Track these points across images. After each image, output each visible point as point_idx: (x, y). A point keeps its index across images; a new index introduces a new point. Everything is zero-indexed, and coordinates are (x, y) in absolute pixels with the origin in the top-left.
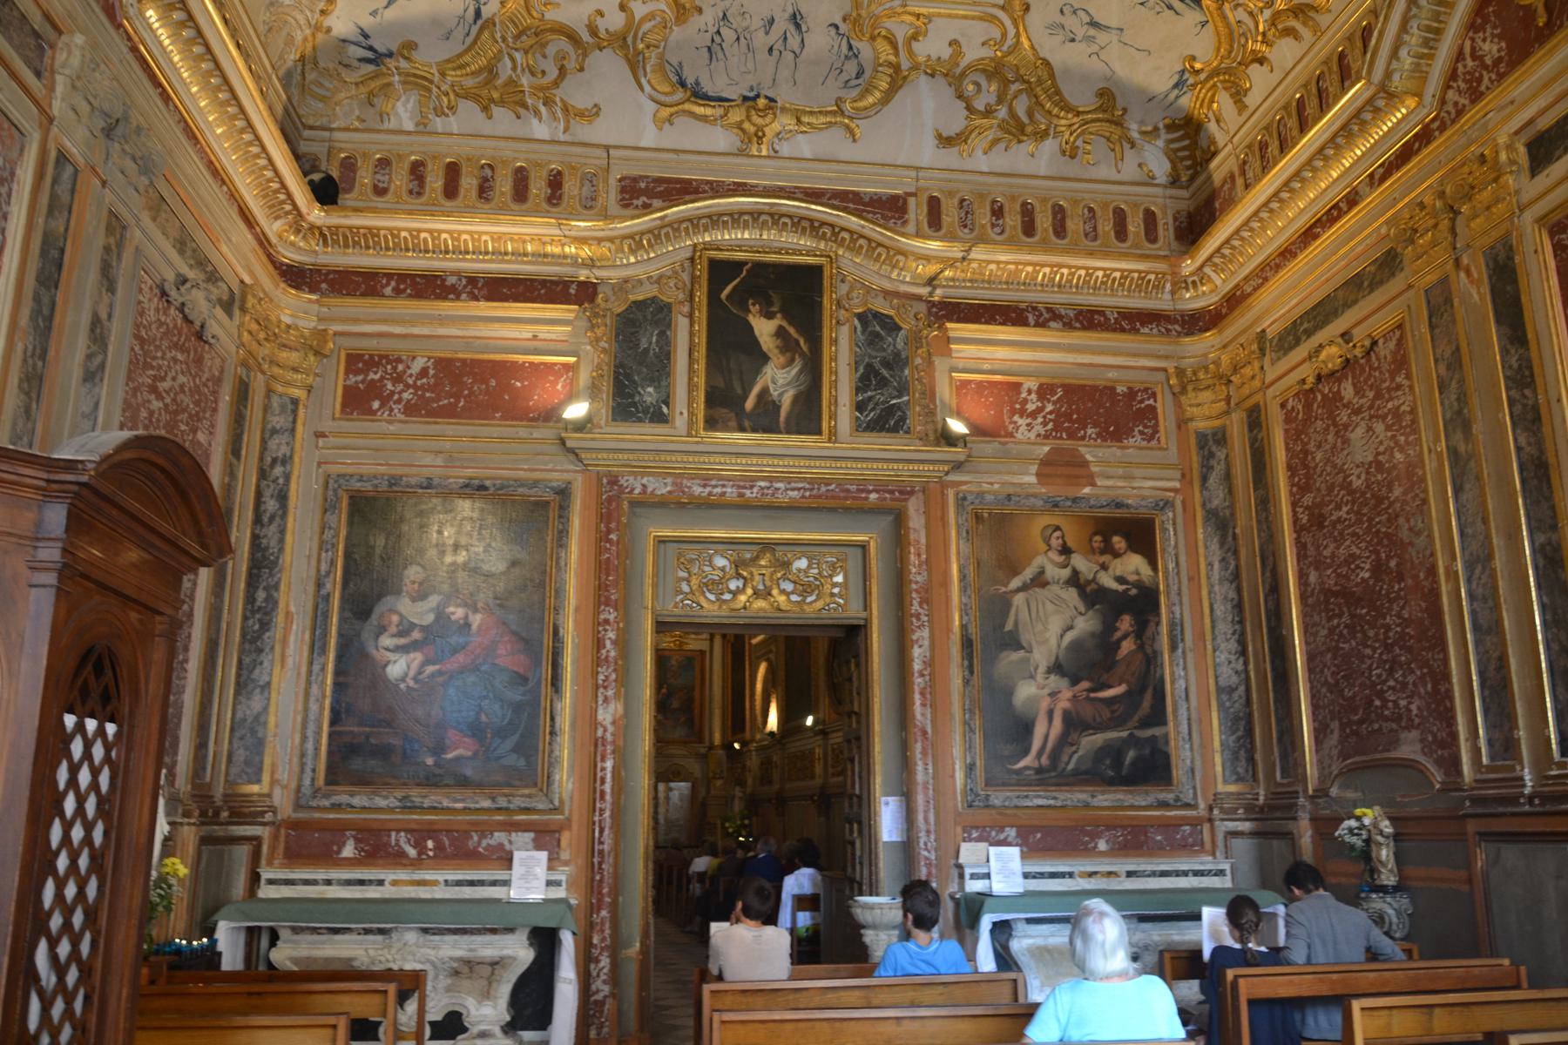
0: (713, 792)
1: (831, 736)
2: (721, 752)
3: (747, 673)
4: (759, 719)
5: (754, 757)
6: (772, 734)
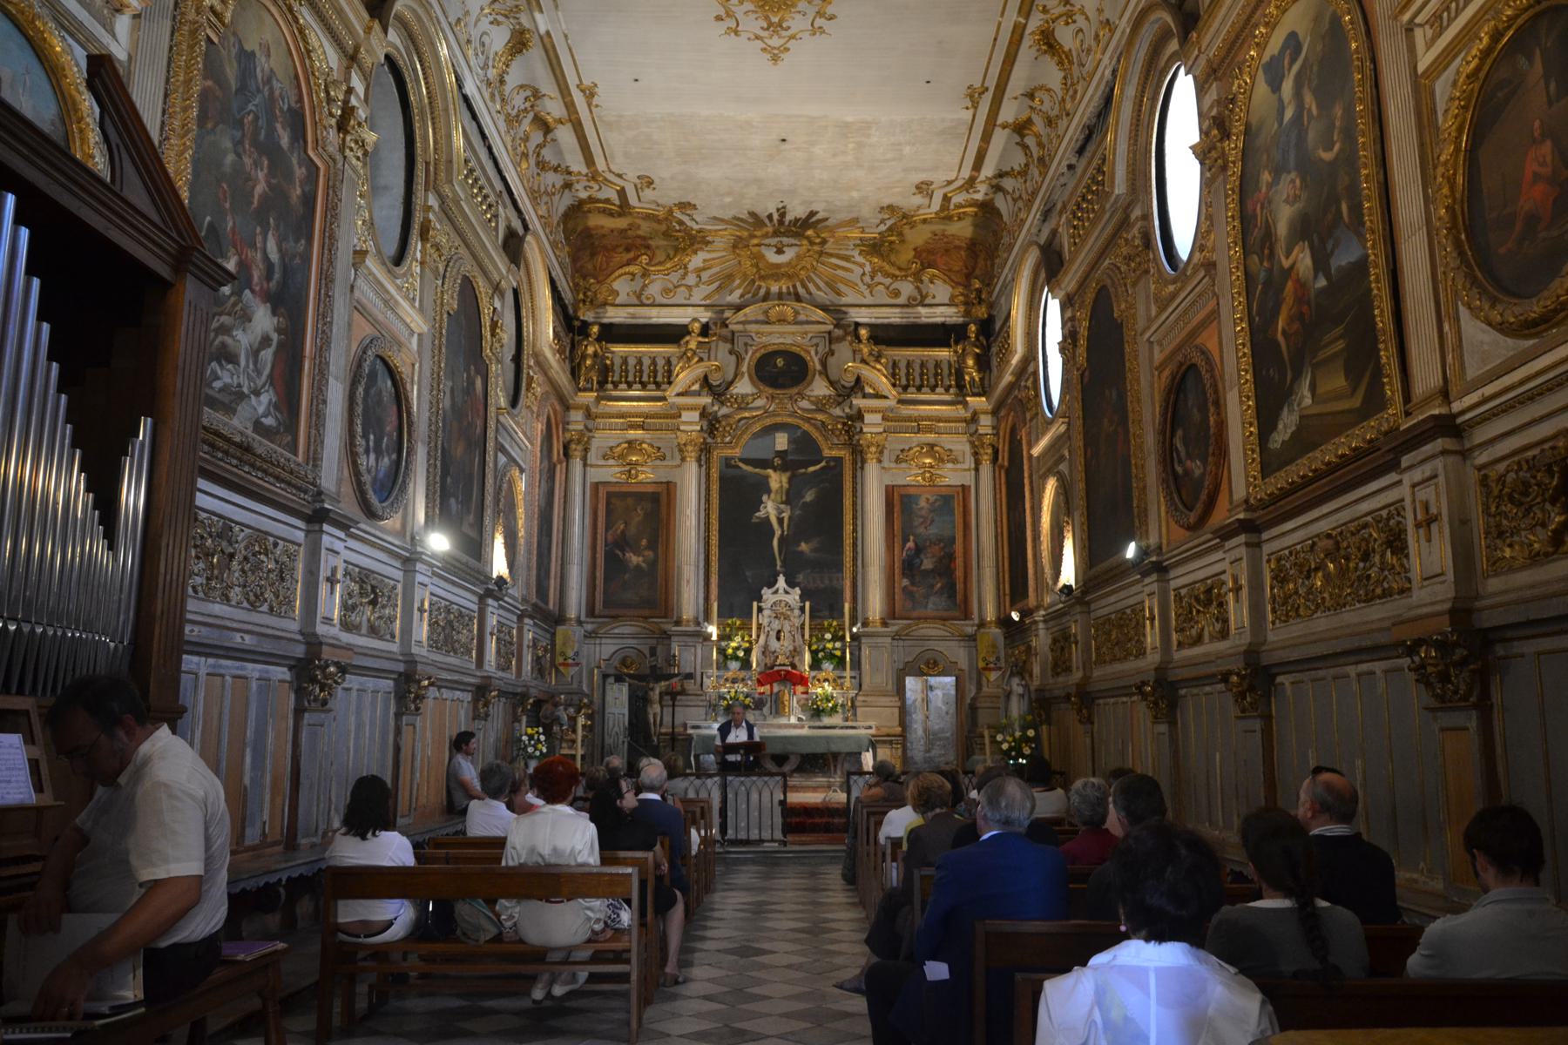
0: (985, 689)
1: (1172, 574)
2: (997, 630)
3: (1028, 506)
4: (1048, 571)
5: (1042, 632)
6: (1067, 588)
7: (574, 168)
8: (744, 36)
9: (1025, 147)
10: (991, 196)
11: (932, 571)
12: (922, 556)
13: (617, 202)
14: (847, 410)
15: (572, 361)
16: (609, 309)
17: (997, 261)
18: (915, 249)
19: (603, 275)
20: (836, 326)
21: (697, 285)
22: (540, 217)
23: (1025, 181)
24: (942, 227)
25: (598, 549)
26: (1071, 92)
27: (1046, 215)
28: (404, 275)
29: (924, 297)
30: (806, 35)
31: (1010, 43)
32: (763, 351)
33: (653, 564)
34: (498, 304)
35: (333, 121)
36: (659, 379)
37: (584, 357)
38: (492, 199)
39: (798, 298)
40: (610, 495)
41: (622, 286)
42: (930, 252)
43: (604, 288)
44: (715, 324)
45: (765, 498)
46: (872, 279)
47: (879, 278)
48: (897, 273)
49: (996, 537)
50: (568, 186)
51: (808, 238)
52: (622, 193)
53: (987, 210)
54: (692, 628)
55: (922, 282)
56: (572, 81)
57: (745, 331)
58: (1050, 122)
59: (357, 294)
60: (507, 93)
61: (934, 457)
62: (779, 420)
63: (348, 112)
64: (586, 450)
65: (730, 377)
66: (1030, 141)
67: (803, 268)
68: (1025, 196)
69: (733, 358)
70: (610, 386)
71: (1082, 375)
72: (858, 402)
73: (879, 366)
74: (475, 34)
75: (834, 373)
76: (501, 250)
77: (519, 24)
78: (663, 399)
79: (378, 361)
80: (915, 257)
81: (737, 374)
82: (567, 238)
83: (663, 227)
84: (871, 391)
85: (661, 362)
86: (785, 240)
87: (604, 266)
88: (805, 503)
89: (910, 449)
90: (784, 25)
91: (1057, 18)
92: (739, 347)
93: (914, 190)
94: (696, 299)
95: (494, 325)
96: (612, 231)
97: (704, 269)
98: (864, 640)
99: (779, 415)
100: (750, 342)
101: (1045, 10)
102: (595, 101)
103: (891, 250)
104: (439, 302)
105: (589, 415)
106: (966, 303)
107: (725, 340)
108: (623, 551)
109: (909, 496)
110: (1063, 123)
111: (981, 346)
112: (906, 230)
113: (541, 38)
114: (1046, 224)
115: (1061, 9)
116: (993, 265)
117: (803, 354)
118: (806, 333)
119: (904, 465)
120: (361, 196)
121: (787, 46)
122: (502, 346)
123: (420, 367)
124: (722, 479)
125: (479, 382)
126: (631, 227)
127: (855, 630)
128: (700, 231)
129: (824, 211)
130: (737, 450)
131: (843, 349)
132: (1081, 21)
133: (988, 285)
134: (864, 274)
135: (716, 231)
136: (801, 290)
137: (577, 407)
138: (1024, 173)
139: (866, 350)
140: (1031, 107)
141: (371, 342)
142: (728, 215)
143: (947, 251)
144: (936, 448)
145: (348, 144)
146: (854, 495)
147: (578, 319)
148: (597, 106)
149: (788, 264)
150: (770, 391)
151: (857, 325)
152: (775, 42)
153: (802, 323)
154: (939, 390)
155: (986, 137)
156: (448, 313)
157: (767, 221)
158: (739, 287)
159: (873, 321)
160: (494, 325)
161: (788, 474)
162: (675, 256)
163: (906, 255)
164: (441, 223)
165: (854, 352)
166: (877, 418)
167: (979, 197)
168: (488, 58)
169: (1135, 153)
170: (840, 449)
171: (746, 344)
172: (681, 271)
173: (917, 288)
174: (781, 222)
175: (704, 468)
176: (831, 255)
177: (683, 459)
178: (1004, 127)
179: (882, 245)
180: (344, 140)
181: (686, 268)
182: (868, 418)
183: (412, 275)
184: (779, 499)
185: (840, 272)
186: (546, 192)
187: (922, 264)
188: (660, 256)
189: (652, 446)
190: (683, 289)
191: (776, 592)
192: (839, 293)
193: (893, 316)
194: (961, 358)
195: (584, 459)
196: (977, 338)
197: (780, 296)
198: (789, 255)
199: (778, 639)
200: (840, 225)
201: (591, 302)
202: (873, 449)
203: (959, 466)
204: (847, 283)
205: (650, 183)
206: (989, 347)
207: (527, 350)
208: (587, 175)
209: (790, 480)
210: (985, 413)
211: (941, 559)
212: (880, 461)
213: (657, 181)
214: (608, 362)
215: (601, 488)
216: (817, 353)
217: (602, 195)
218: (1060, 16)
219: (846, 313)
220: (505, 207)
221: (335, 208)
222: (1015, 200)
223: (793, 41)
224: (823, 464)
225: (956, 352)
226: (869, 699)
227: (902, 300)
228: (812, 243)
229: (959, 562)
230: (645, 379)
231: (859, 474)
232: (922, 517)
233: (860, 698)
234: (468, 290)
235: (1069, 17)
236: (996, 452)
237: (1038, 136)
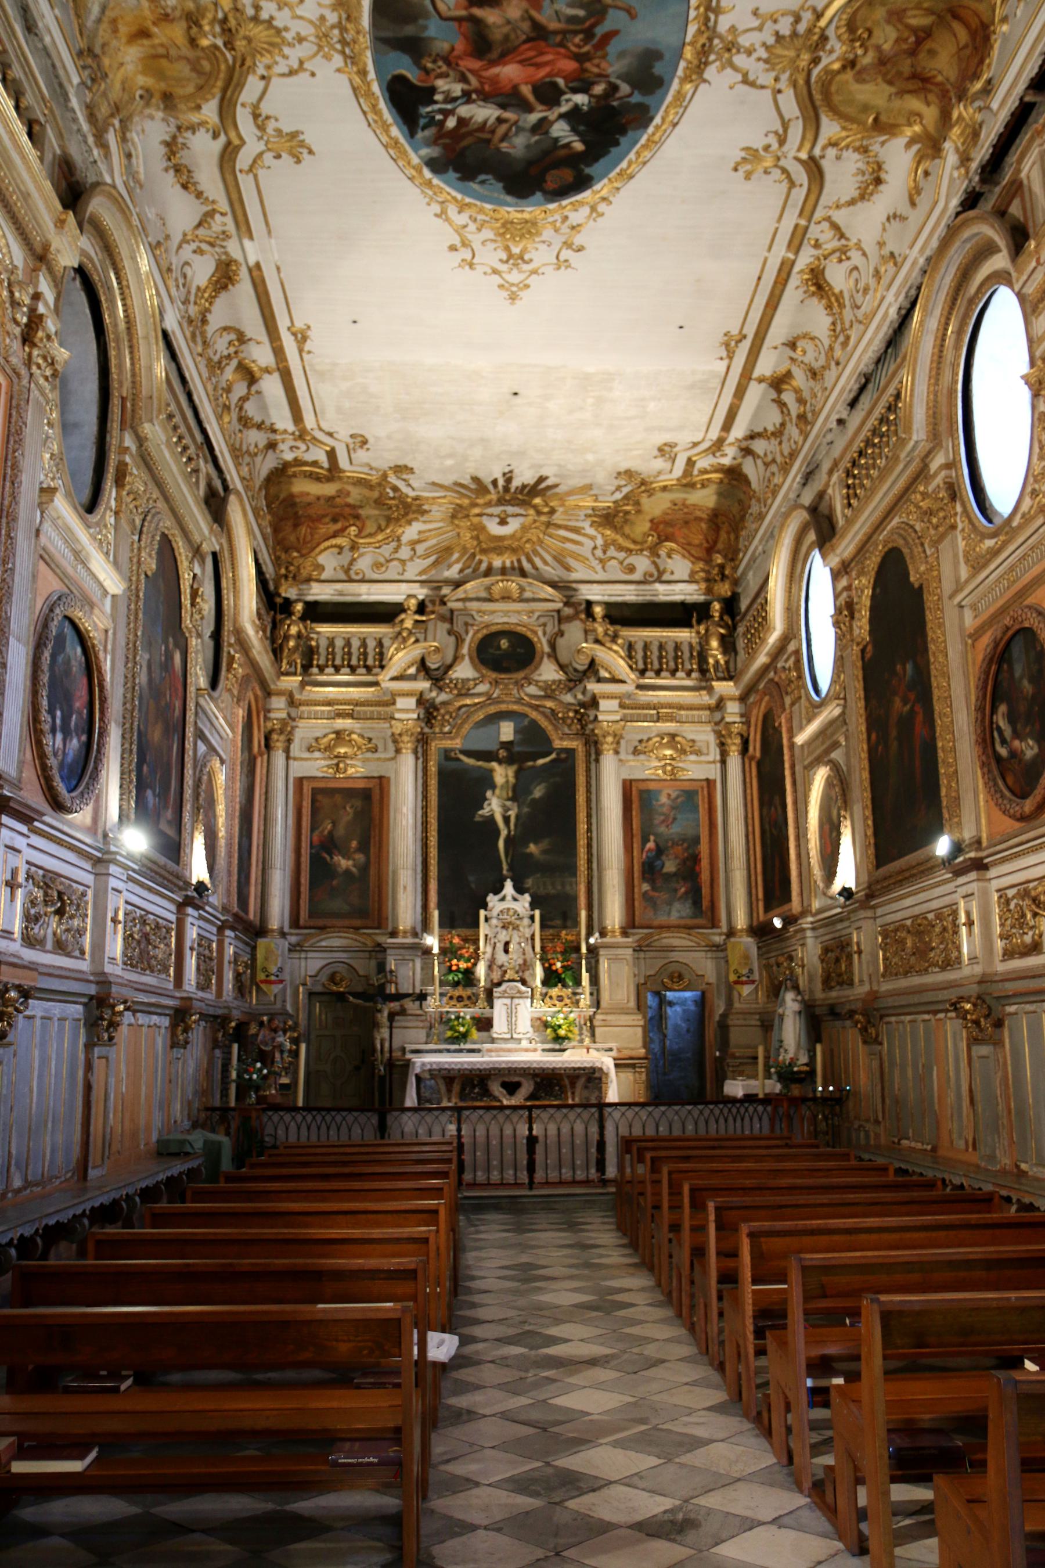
0: (737, 1005)
1: (993, 872)
2: (750, 939)
3: (789, 800)
4: (817, 872)
5: (810, 941)
6: (846, 892)
7: (280, 426)
8: (480, 269)
9: (782, 405)
10: (739, 460)
11: (675, 874)
12: (664, 858)
13: (326, 465)
14: (580, 696)
15: (273, 641)
16: (314, 585)
17: (743, 533)
18: (652, 521)
19: (307, 548)
20: (566, 604)
21: (411, 559)
22: (243, 479)
23: (780, 443)
24: (682, 496)
25: (303, 851)
26: (841, 339)
27: (808, 477)
28: (98, 524)
29: (661, 573)
30: (549, 270)
31: (776, 282)
32: (485, 632)
33: (365, 869)
34: (197, 570)
35: (17, 331)
36: (370, 662)
37: (287, 637)
38: (192, 451)
39: (523, 574)
40: (315, 792)
41: (328, 560)
42: (668, 523)
43: (308, 563)
44: (433, 602)
45: (489, 794)
46: (605, 552)
47: (612, 552)
48: (632, 546)
49: (747, 836)
50: (272, 446)
51: (535, 507)
52: (332, 454)
53: (734, 475)
54: (409, 940)
55: (659, 556)
56: (282, 323)
57: (465, 609)
58: (814, 374)
59: (43, 540)
60: (209, 335)
61: (675, 749)
62: (503, 707)
63: (35, 321)
64: (289, 741)
65: (449, 660)
66: (788, 397)
67: (528, 541)
68: (779, 459)
69: (452, 639)
70: (315, 670)
71: (863, 651)
72: (593, 687)
73: (615, 647)
74: (176, 262)
75: (564, 656)
76: (204, 506)
77: (226, 253)
78: (376, 684)
79: (67, 623)
80: (651, 529)
81: (456, 658)
82: (268, 506)
83: (376, 494)
84: (607, 675)
85: (371, 644)
86: (510, 509)
87: (309, 538)
88: (534, 800)
89: (649, 739)
90: (526, 257)
91: (830, 254)
92: (459, 627)
93: (656, 453)
94: (409, 575)
95: (194, 594)
96: (318, 498)
97: (419, 541)
98: (602, 952)
99: (503, 702)
100: (471, 621)
101: (817, 245)
102: (307, 346)
103: (626, 521)
104: (135, 560)
105: (292, 702)
106: (707, 580)
107: (442, 618)
108: (330, 854)
109: (648, 791)
110: (830, 375)
111: (726, 626)
112: (644, 500)
113: (250, 270)
114: (807, 488)
115: (836, 244)
116: (737, 538)
117: (529, 634)
118: (532, 612)
119: (642, 757)
120: (50, 424)
121: (527, 282)
122: (202, 618)
123: (114, 634)
124: (441, 773)
125: (177, 658)
126: (340, 493)
127: (592, 941)
128: (416, 499)
129: (555, 476)
130: (458, 741)
131: (574, 630)
132: (856, 258)
133: (732, 560)
134: (595, 548)
135: (434, 498)
136: (526, 566)
137: (280, 693)
138: (778, 433)
139: (600, 630)
140: (792, 359)
141: (59, 598)
142: (448, 480)
143: (686, 523)
144: (678, 739)
145: (34, 359)
146: (588, 791)
147: (279, 595)
148: (309, 352)
149: (512, 536)
150: (494, 675)
151: (589, 604)
152: (515, 277)
153: (527, 600)
154: (680, 674)
155: (740, 392)
156: (146, 575)
157: (491, 487)
158: (457, 561)
159: (606, 599)
160: (194, 594)
161: (514, 767)
162: (387, 526)
163: (641, 527)
164: (138, 469)
165: (586, 632)
166: (614, 704)
167: (726, 461)
168: (189, 292)
169: (936, 395)
170: (572, 740)
171: (466, 624)
172: (394, 544)
173: (654, 563)
174: (506, 489)
175: (420, 761)
176: (559, 527)
177: (398, 751)
178: (760, 380)
179: (615, 516)
180: (30, 355)
181: (399, 540)
182: (604, 704)
183: (106, 526)
184: (505, 795)
185: (569, 546)
186: (248, 452)
187: (659, 537)
188: (370, 527)
189: (362, 737)
190: (395, 563)
191: (503, 899)
192: (568, 569)
193: (629, 594)
194: (704, 640)
195: (287, 751)
196: (721, 618)
197: (503, 571)
198: (514, 526)
199: (506, 951)
200: (571, 493)
201: (294, 578)
202: (610, 739)
203: (703, 758)
204: (577, 557)
205: (365, 442)
206: (735, 627)
207: (228, 626)
208: (293, 434)
209: (517, 775)
210: (732, 699)
211: (684, 862)
212: (617, 752)
213: (371, 440)
214: (313, 643)
215: (305, 783)
216: (545, 634)
217: (309, 457)
218: (834, 252)
219: (575, 590)
220: (206, 462)
221: (19, 432)
222: (767, 465)
223: (534, 276)
224: (553, 756)
225: (698, 633)
226: (609, 1017)
227: (637, 576)
228: (539, 513)
229: (705, 863)
230: (354, 662)
231: (593, 766)
232: (663, 814)
233: (598, 1017)
234: (166, 550)
235: (843, 253)
236: (745, 743)
237: (797, 391)
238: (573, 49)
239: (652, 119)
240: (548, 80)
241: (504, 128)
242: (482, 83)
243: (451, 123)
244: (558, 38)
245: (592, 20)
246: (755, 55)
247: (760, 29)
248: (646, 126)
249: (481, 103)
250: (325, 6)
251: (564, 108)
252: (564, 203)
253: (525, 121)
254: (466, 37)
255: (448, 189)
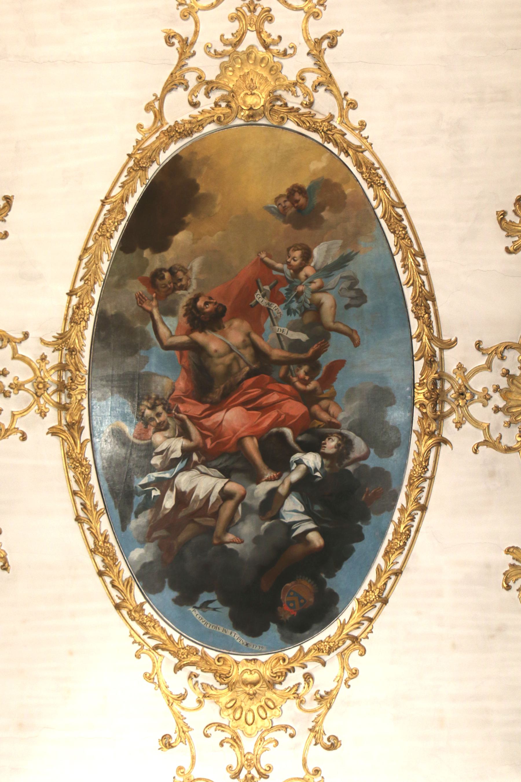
238: (299, 385)
239: (395, 497)
240: (274, 430)
241: (230, 505)
242: (204, 437)
243: (169, 502)
244: (282, 370)
245: (315, 347)
246: (491, 404)
247: (489, 367)
248: (391, 508)
249: (202, 468)
250: (47, 344)
251: (295, 476)
252: (307, 645)
253: (252, 497)
254: (187, 371)
255: (163, 624)
